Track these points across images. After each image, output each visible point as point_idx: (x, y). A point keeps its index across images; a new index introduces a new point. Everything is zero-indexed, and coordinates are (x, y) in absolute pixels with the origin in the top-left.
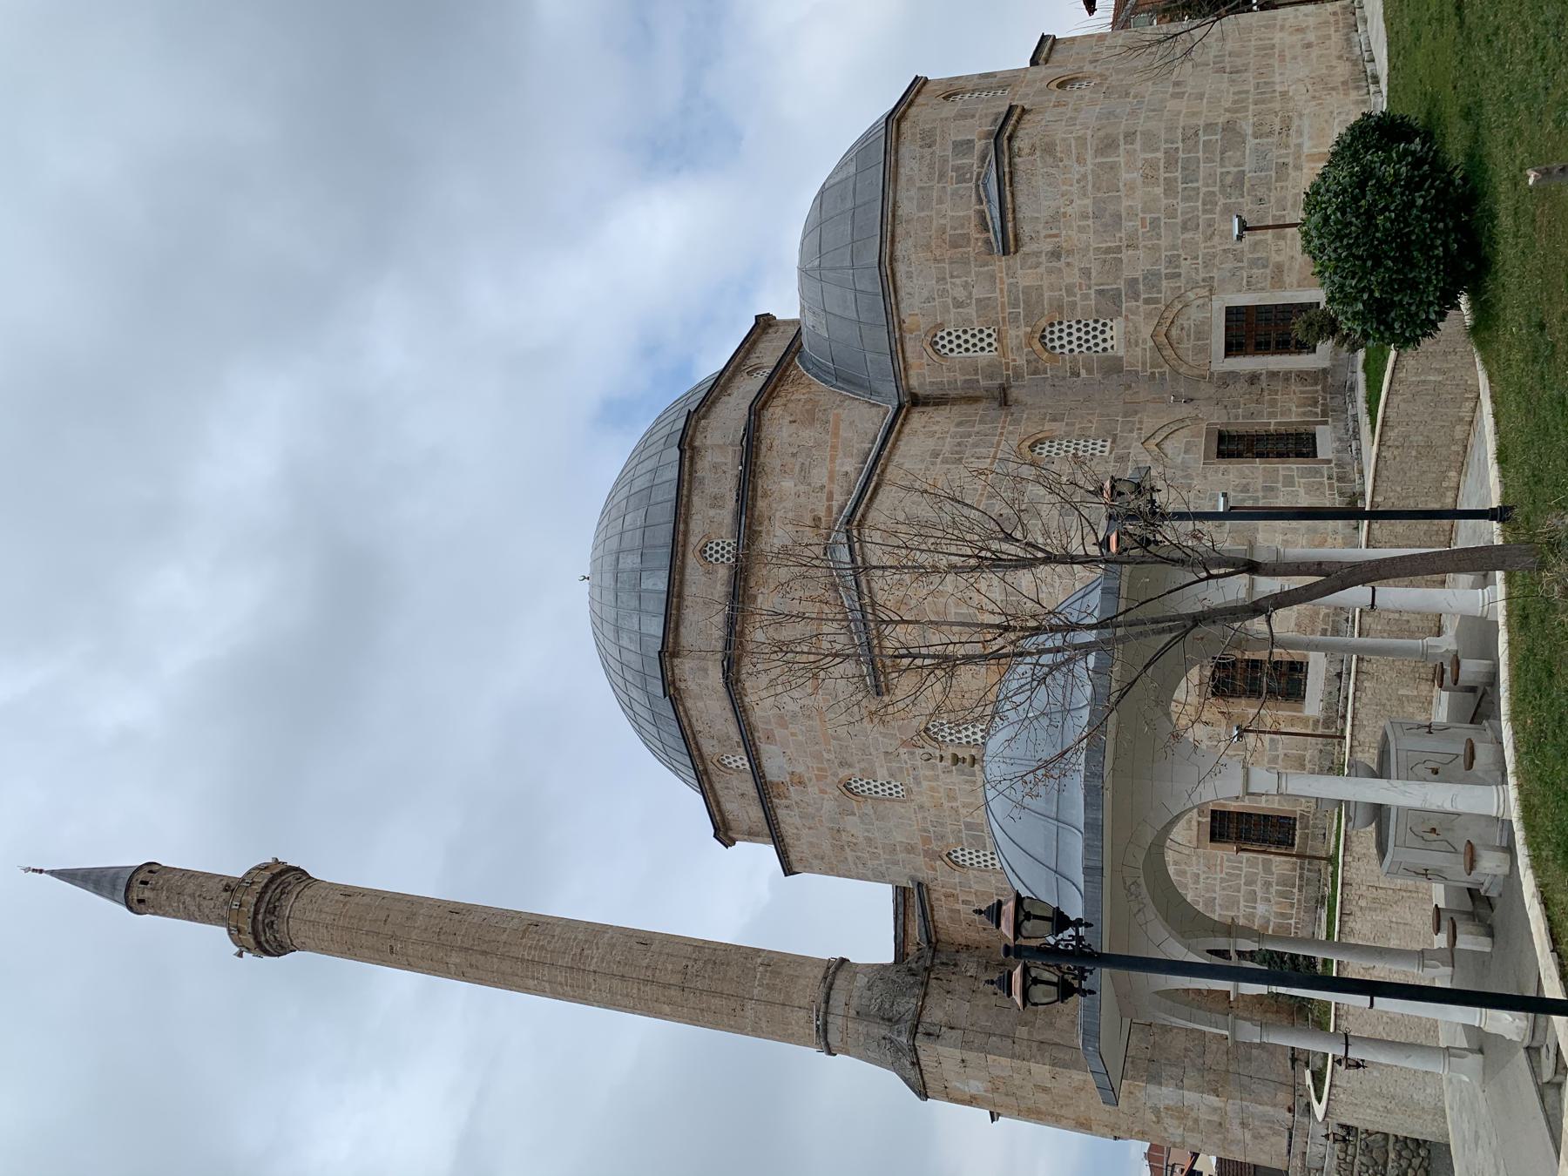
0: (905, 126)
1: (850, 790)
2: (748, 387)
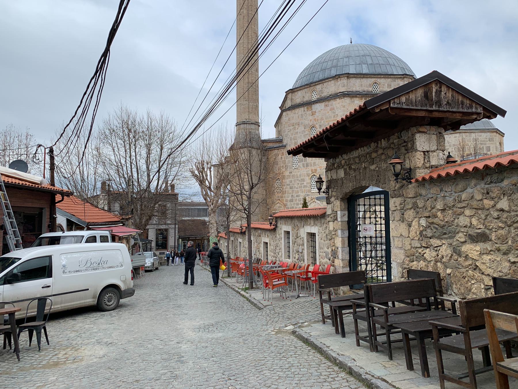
0: (495, 134)
1: (312, 128)
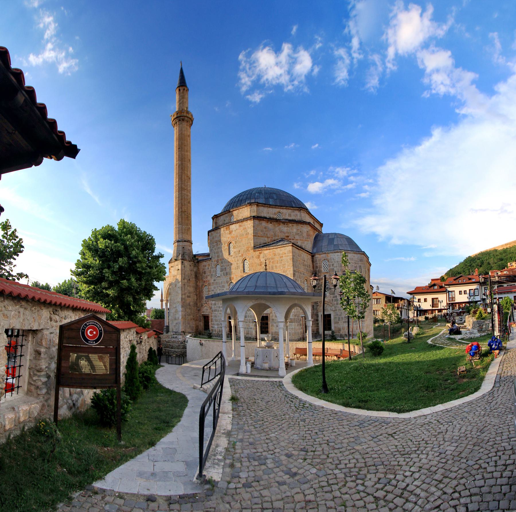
2: (312, 221)
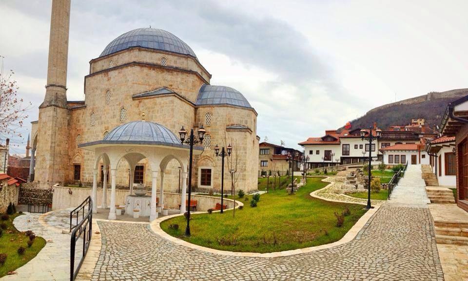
2: (199, 72)
